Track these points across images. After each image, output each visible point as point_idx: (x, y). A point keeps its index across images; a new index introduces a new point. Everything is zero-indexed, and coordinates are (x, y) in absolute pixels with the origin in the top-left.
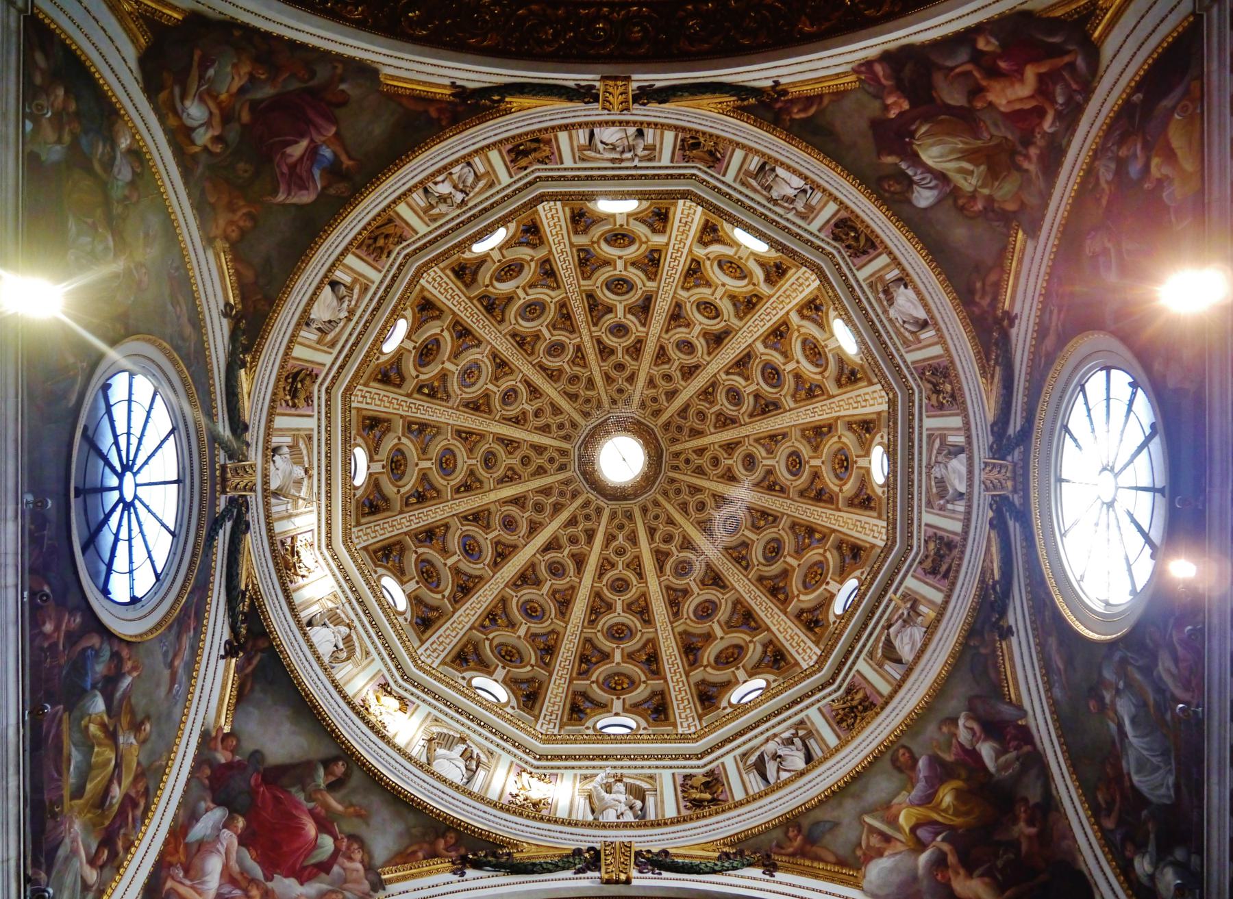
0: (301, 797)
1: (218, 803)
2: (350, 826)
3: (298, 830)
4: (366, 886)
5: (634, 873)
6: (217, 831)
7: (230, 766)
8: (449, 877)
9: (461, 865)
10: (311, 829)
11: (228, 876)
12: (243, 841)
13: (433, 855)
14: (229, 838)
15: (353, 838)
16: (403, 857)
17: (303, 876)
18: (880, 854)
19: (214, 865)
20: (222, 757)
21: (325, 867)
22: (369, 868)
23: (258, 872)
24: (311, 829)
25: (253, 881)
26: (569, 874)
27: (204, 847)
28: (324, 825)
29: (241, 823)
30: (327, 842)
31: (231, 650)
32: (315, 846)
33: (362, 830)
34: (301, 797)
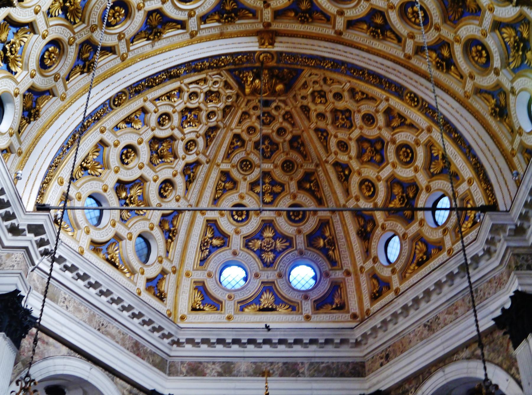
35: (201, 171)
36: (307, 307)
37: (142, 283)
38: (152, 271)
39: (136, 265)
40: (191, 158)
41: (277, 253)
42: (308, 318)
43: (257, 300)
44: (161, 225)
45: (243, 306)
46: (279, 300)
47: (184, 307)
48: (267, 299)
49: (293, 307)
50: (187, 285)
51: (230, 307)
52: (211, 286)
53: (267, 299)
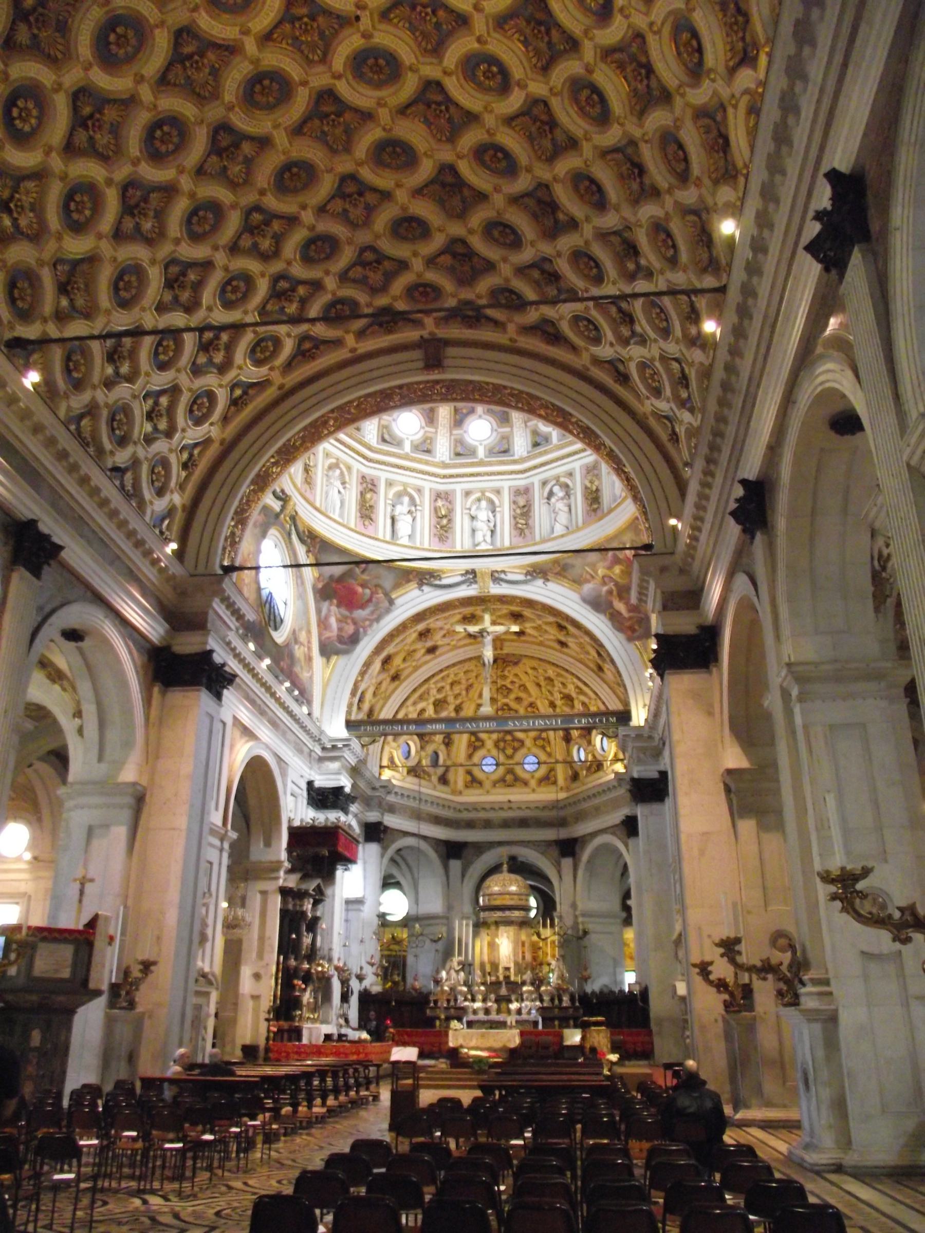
0: (352, 581)
1: (325, 600)
2: (375, 582)
3: (355, 593)
4: (386, 604)
5: (491, 585)
6: (329, 611)
7: (324, 587)
8: (416, 592)
9: (421, 584)
10: (360, 590)
11: (339, 621)
12: (338, 606)
13: (409, 581)
14: (334, 609)
15: (377, 586)
16: (397, 586)
17: (363, 606)
18: (588, 581)
19: (333, 621)
20: (320, 585)
21: (370, 600)
22: (387, 595)
23: (346, 613)
24: (360, 590)
25: (346, 617)
26: (464, 587)
27: (327, 617)
28: (363, 586)
29: (335, 601)
30: (368, 591)
31: (308, 551)
32: (364, 594)
33: (381, 582)
34: (352, 581)
35: (465, 706)
36: (533, 783)
37: (435, 779)
38: (440, 771)
39: (431, 770)
40: (458, 702)
41: (515, 750)
42: (534, 791)
43: (503, 780)
44: (444, 742)
45: (495, 784)
46: (517, 779)
47: (460, 785)
48: (509, 778)
49: (526, 783)
50: (461, 771)
51: (487, 784)
52: (476, 772)
53: (509, 778)
